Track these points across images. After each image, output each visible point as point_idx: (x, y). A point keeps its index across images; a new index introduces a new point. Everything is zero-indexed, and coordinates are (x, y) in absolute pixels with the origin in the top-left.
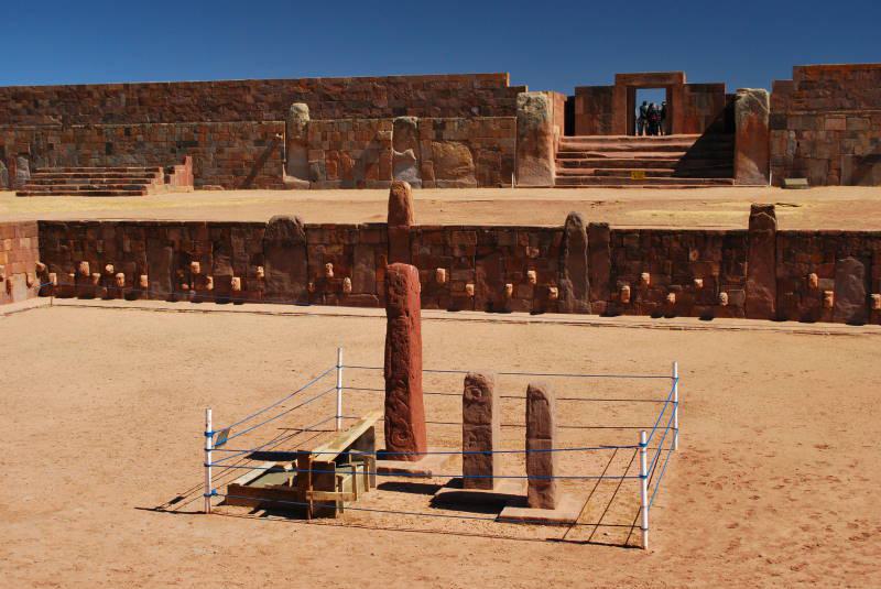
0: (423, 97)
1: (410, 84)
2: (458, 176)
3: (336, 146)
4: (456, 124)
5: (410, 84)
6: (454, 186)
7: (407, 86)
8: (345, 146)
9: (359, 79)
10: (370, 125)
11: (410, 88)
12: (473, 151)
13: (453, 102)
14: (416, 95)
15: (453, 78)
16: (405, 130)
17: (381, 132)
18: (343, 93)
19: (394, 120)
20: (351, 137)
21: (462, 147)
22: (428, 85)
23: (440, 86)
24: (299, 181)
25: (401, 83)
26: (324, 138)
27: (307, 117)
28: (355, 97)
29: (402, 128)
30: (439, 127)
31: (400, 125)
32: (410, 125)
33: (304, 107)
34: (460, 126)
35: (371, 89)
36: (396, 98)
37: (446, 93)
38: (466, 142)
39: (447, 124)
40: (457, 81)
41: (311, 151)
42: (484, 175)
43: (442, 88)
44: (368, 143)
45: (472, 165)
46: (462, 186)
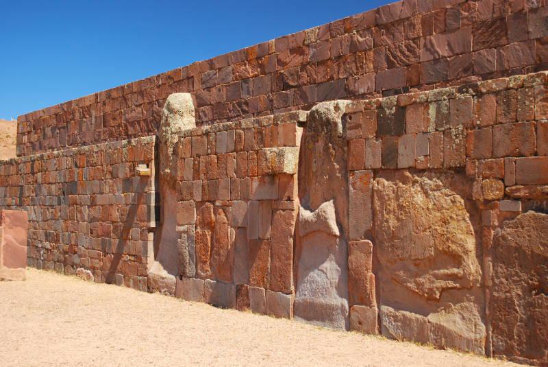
0: (443, 51)
1: (417, 21)
2: (431, 302)
4: (432, 110)
5: (417, 21)
6: (421, 340)
7: (412, 25)
11: (419, 29)
12: (476, 210)
14: (430, 49)
18: (303, 67)
19: (303, 116)
20: (232, 163)
21: (450, 201)
24: (164, 273)
25: (401, 21)
27: (186, 123)
30: (391, 126)
31: (317, 126)
34: (442, 119)
35: (345, 50)
36: (391, 65)
38: (457, 176)
39: (410, 116)
42: (508, 304)
43: (487, 16)
44: (255, 184)
45: (472, 265)
46: (444, 340)
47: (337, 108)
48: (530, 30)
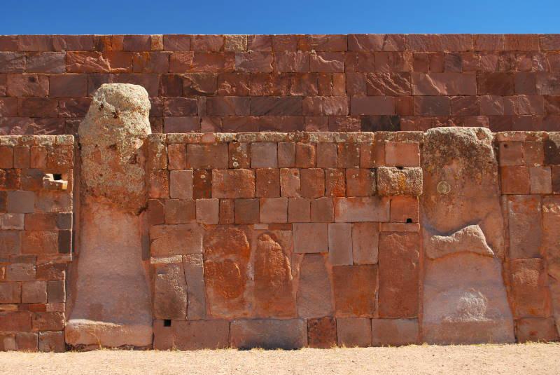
0: (441, 89)
1: (407, 57)
3: (237, 217)
8: (271, 210)
9: (269, 40)
10: (351, 146)
11: (408, 66)
13: (521, 103)
14: (423, 85)
15: (520, 44)
16: (457, 167)
17: (391, 172)
20: (291, 182)
22: (457, 58)
23: (488, 64)
26: (203, 188)
27: (144, 124)
28: (256, 89)
29: (448, 157)
32: (468, 150)
33: (138, 94)
37: (500, 84)
40: (530, 55)
41: (157, 229)
47: (480, 133)
48: (538, 87)
